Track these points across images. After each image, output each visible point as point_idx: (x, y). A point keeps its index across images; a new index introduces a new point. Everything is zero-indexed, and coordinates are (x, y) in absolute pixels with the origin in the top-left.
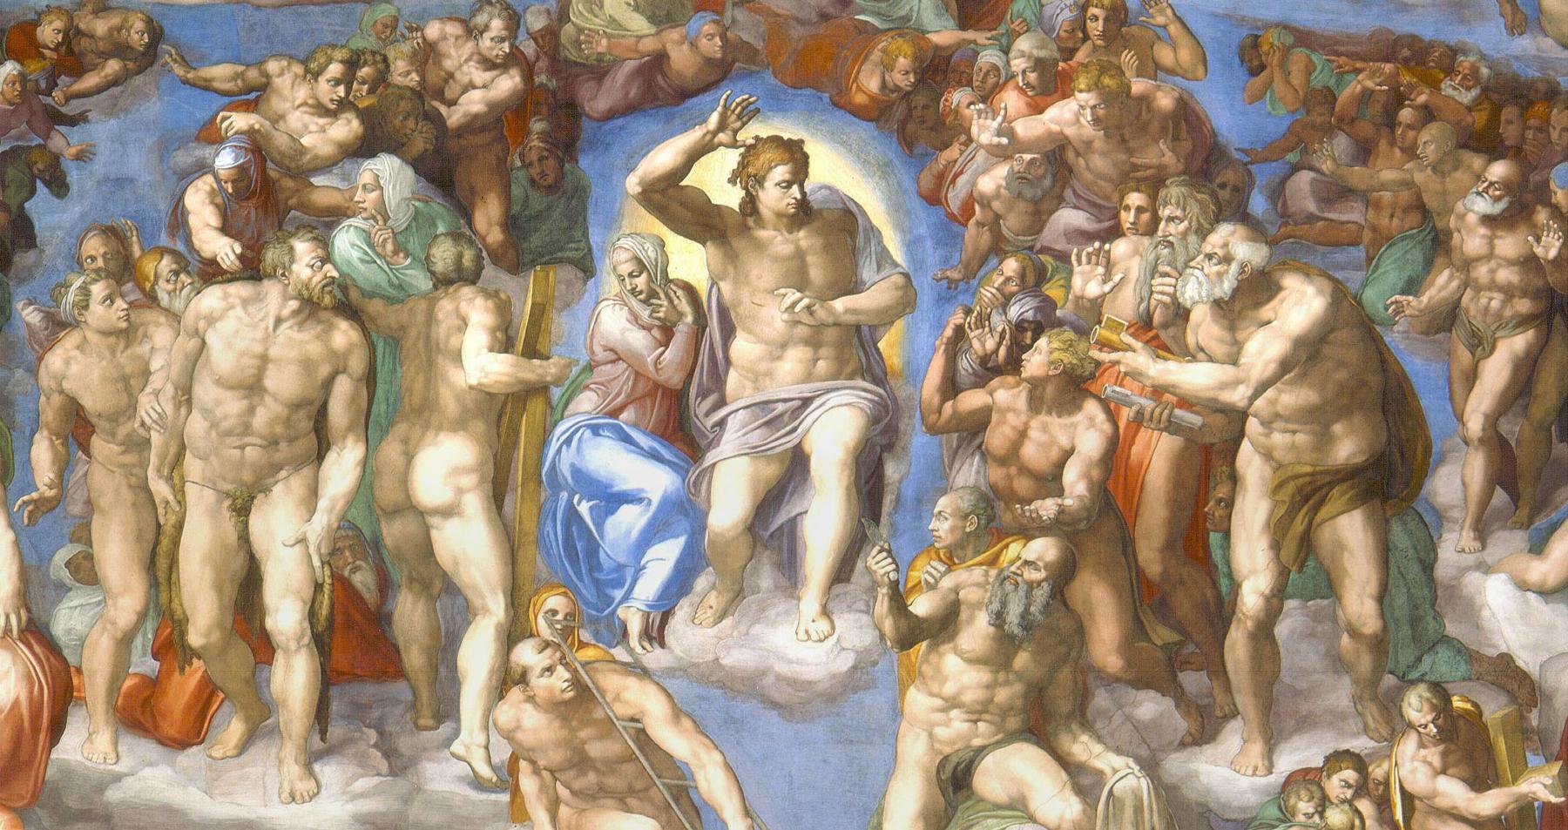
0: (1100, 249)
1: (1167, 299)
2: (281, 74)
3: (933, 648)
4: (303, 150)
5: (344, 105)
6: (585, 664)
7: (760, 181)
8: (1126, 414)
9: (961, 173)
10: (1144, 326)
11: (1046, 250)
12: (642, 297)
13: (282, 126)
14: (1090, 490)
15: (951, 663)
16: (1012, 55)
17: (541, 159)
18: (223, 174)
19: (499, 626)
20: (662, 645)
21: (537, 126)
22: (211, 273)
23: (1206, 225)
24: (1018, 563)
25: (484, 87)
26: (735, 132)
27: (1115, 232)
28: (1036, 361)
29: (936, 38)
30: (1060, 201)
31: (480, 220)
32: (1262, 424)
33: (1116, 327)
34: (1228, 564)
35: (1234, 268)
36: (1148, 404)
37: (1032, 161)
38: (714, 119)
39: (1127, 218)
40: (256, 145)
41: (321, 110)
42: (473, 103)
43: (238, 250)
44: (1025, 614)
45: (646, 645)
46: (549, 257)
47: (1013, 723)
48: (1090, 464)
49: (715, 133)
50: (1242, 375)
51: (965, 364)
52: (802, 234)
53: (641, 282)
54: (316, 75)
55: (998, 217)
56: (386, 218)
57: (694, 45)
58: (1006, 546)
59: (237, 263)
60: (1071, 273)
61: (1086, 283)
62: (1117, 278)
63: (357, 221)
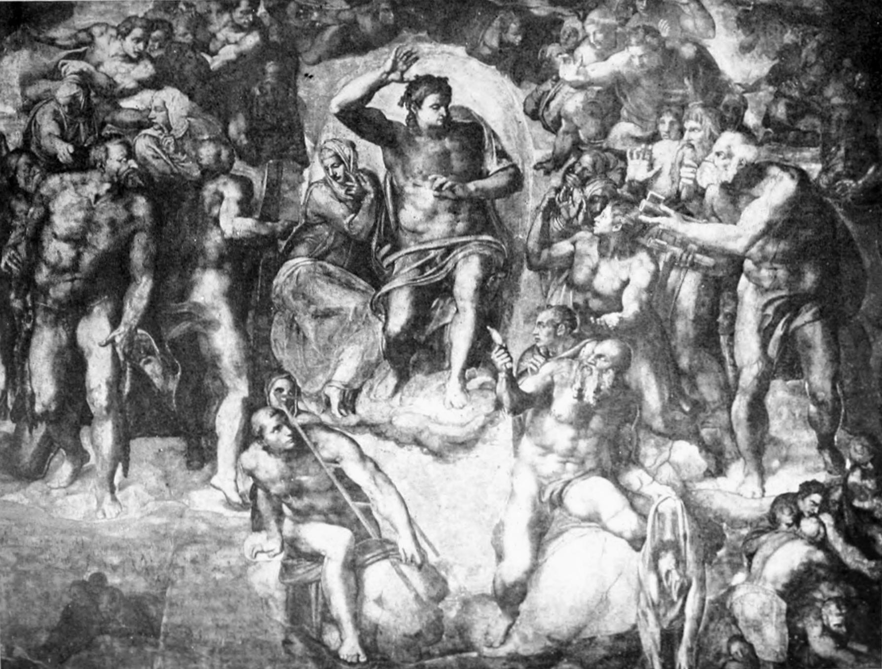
0: (645, 149)
1: (691, 182)
2: (102, 34)
3: (536, 414)
4: (114, 85)
5: (141, 56)
6: (303, 427)
7: (419, 103)
8: (665, 257)
9: (552, 99)
10: (676, 202)
11: (608, 149)
12: (341, 180)
13: (102, 69)
14: (641, 308)
15: (548, 422)
16: (587, 21)
17: (273, 89)
18: (61, 101)
19: (245, 400)
20: (354, 412)
21: (271, 68)
22: (54, 166)
23: (716, 133)
24: (593, 357)
25: (236, 43)
26: (403, 72)
27: (655, 138)
28: (605, 222)
29: (536, 12)
30: (617, 118)
31: (232, 129)
32: (756, 264)
33: (657, 201)
34: (732, 356)
35: (735, 161)
36: (678, 251)
37: (599, 92)
38: (389, 65)
39: (663, 128)
40: (85, 81)
41: (127, 58)
42: (228, 53)
43: (71, 149)
44: (598, 390)
45: (343, 411)
46: (280, 155)
47: (590, 464)
48: (640, 291)
49: (389, 73)
50: (742, 232)
51: (556, 225)
52: (447, 140)
53: (340, 171)
54: (124, 36)
55: (577, 128)
56: (170, 128)
57: (375, 16)
58: (584, 346)
59: (70, 159)
60: (626, 164)
61: (636, 170)
62: (656, 168)
63: (150, 131)
